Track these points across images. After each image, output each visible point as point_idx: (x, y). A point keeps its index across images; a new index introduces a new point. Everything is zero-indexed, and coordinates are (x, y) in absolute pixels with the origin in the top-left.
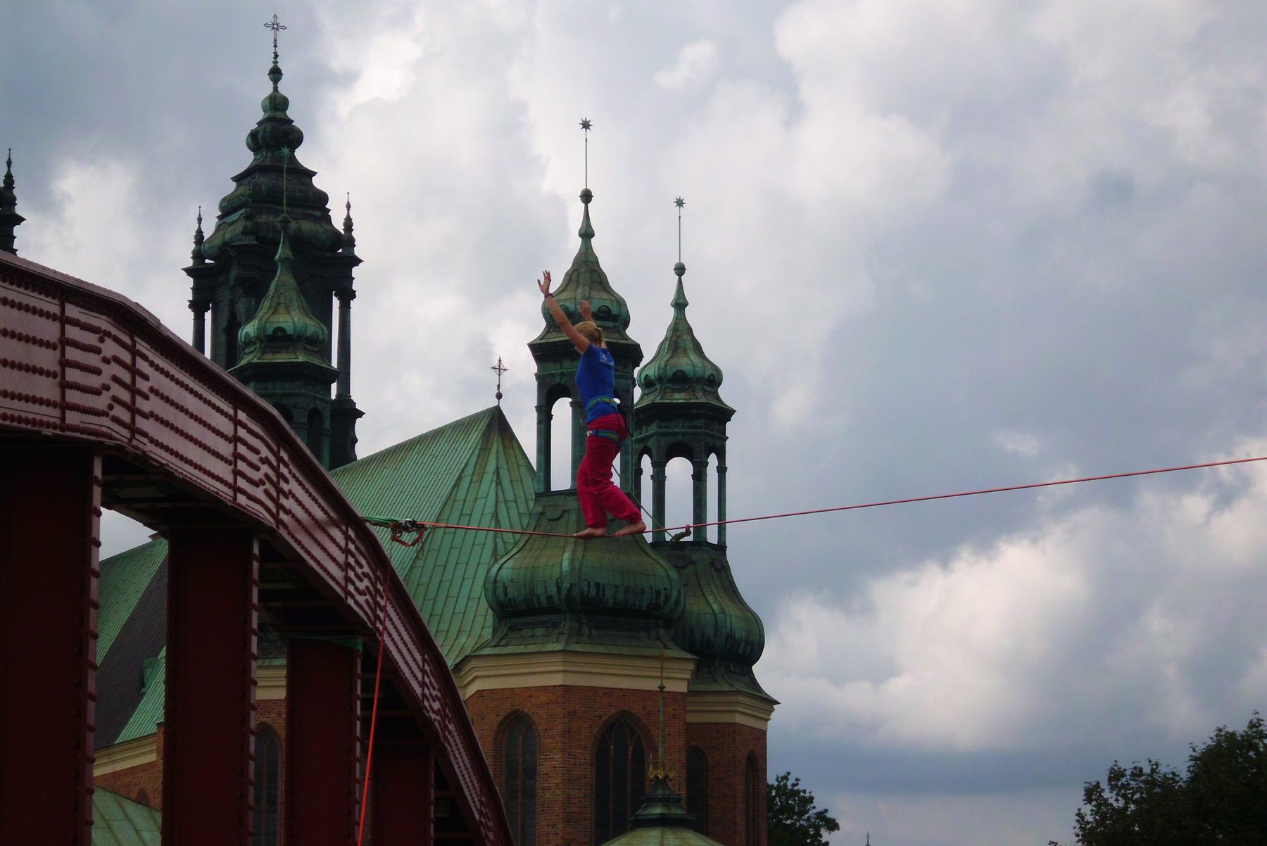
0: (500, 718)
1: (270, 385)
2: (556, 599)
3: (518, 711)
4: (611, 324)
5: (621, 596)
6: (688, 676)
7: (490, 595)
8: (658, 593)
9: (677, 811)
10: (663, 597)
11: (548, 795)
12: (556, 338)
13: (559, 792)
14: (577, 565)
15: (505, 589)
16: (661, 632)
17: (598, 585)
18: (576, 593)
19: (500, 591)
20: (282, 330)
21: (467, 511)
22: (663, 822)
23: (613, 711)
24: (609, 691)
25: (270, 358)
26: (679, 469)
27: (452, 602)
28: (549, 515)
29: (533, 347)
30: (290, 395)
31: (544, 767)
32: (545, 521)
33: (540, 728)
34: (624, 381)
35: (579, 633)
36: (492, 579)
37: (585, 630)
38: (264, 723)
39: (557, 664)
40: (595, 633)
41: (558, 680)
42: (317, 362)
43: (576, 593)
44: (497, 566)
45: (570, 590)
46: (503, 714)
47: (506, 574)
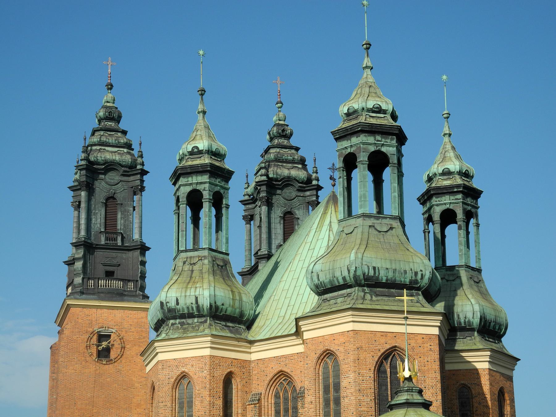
0: (317, 355)
1: (190, 179)
2: (348, 278)
3: (327, 350)
4: (382, 115)
5: (390, 275)
6: (439, 324)
7: (309, 281)
8: (416, 273)
9: (417, 398)
10: (419, 276)
11: (346, 400)
12: (347, 125)
13: (353, 398)
14: (360, 256)
15: (318, 276)
16: (421, 298)
17: (374, 268)
18: (359, 273)
19: (315, 278)
20: (197, 148)
21: (312, 247)
22: (408, 404)
23: (388, 347)
24: (384, 334)
25: (190, 163)
26: (451, 229)
27: (300, 297)
28: (347, 231)
29: (333, 133)
30: (201, 183)
31: (344, 383)
32: (344, 235)
33: (341, 358)
34: (391, 149)
35: (364, 298)
36: (310, 271)
37: (368, 296)
38: (184, 372)
39: (348, 316)
40: (374, 298)
41: (350, 327)
42: (217, 164)
43: (359, 273)
44: (313, 264)
45: (355, 271)
46: (319, 352)
47: (318, 267)
